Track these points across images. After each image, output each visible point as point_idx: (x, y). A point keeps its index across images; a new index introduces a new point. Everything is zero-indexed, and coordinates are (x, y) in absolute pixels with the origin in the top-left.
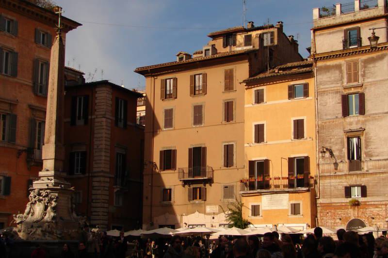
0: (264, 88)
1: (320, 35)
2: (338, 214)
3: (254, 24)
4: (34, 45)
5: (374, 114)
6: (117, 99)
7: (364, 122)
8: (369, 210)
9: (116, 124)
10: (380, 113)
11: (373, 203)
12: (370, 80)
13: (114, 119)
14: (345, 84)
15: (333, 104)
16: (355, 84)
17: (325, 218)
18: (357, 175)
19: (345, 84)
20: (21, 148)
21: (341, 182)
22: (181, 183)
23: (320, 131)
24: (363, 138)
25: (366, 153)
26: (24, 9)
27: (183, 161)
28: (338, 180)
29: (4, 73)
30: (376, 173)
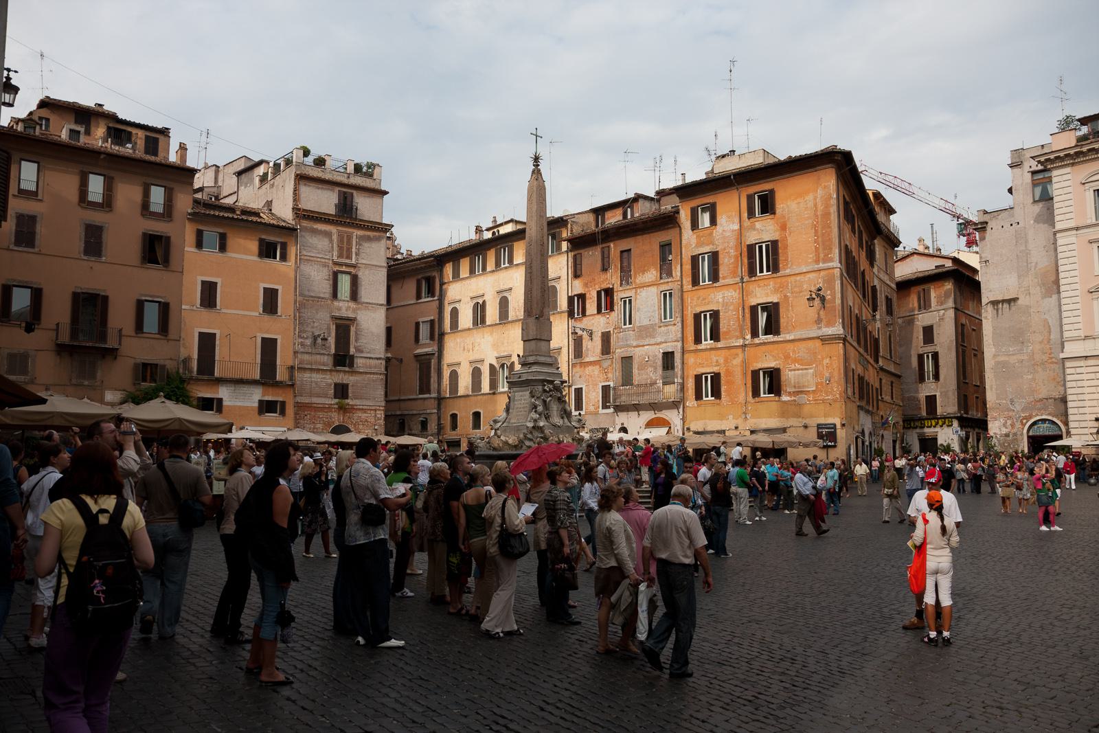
2: (319, 417)
5: (367, 303)
7: (354, 311)
10: (375, 304)
11: (361, 407)
12: (364, 262)
14: (335, 258)
15: (318, 278)
16: (348, 261)
17: (302, 421)
18: (345, 372)
19: (335, 258)
21: (324, 378)
23: (300, 307)
24: (353, 329)
25: (355, 348)
27: (58, 311)
28: (321, 376)
30: (366, 373)
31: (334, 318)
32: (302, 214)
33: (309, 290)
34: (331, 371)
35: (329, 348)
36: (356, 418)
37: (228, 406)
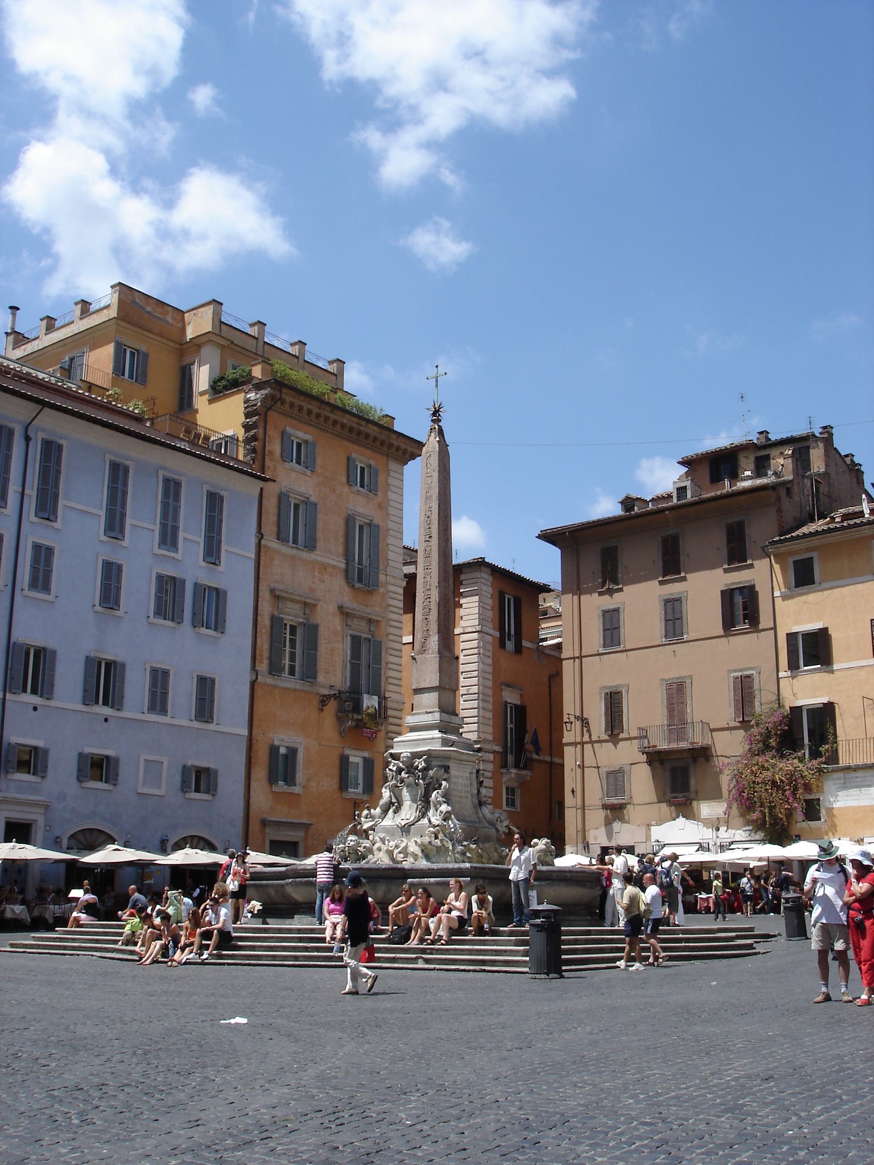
0: (815, 555)
3: (770, 436)
4: (346, 489)
6: (501, 596)
9: (502, 645)
13: (497, 634)
20: (326, 692)
22: (644, 758)
26: (327, 419)
29: (291, 543)
37: (839, 808)
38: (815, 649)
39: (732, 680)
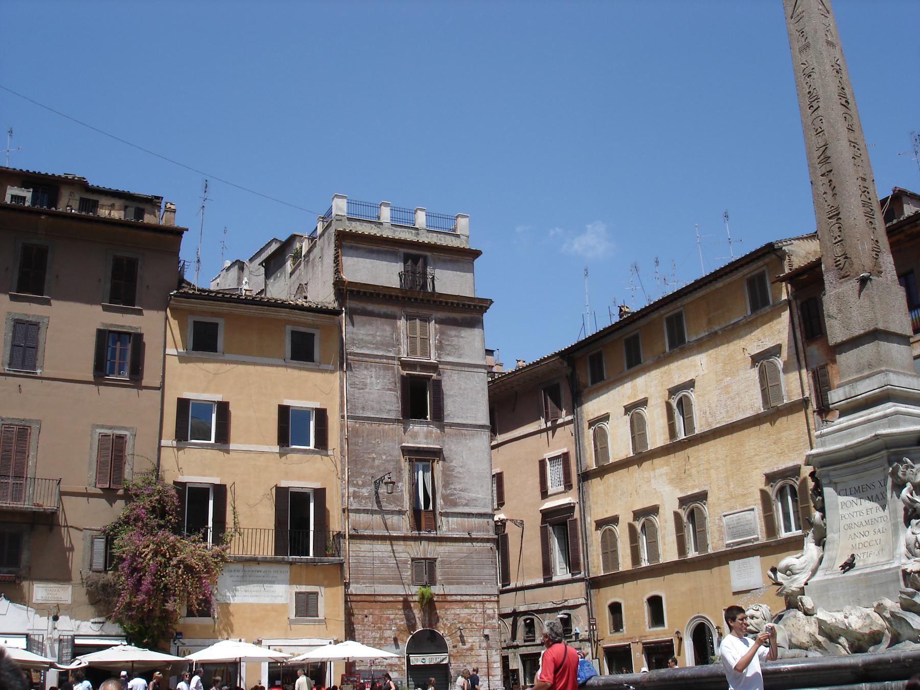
1: (351, 248)
2: (388, 619)
8: (453, 612)
11: (459, 598)
14: (404, 356)
25: (444, 497)
31: (406, 451)
32: (344, 290)
33: (363, 408)
34: (405, 538)
35: (400, 499)
36: (451, 617)
38: (200, 422)
39: (96, 437)
